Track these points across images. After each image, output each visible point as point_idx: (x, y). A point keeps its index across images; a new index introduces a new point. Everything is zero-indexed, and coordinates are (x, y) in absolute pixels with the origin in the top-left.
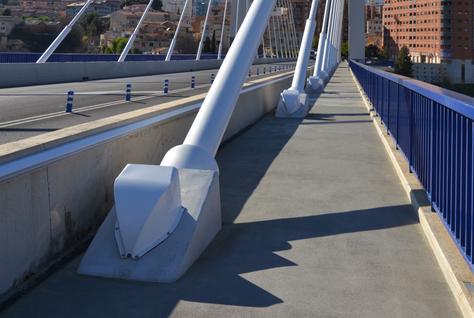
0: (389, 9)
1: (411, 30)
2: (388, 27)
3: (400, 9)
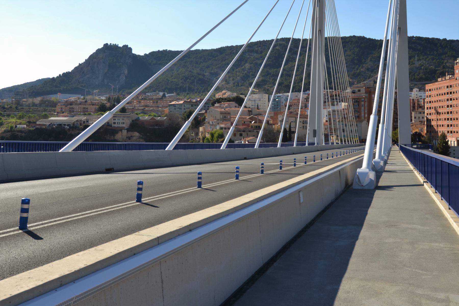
0: (430, 102)
1: (448, 119)
2: (429, 117)
3: (439, 102)
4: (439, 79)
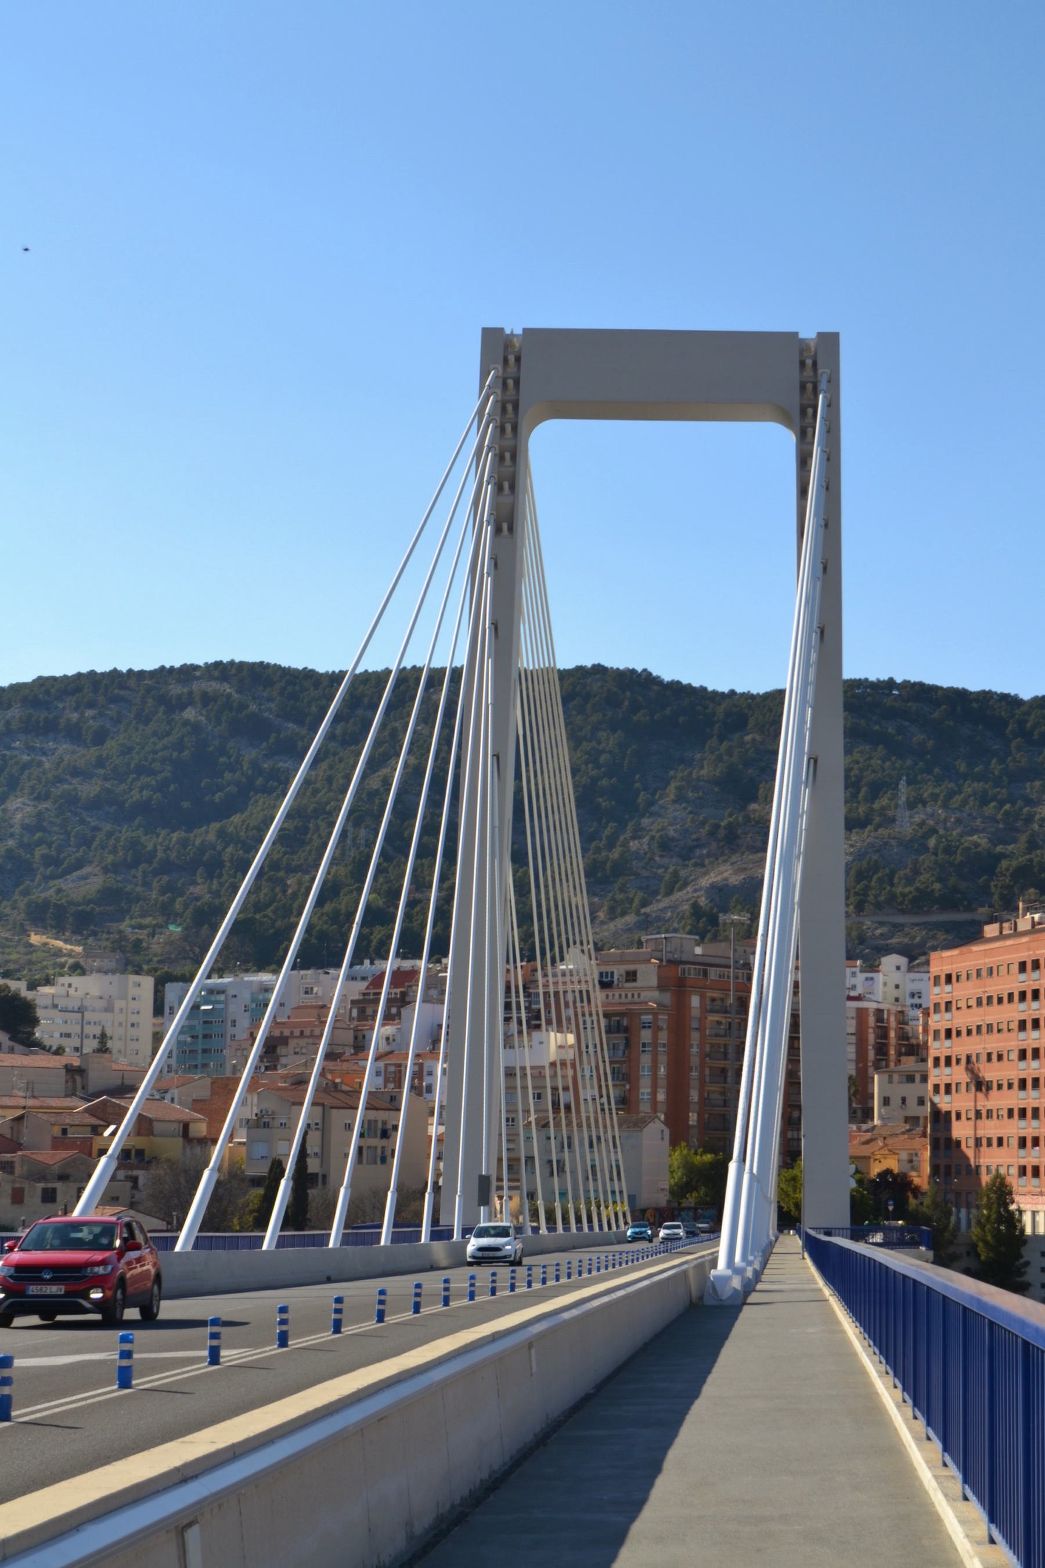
1: (1023, 1113)
2: (944, 1102)
3: (985, 1036)
4: (991, 930)
